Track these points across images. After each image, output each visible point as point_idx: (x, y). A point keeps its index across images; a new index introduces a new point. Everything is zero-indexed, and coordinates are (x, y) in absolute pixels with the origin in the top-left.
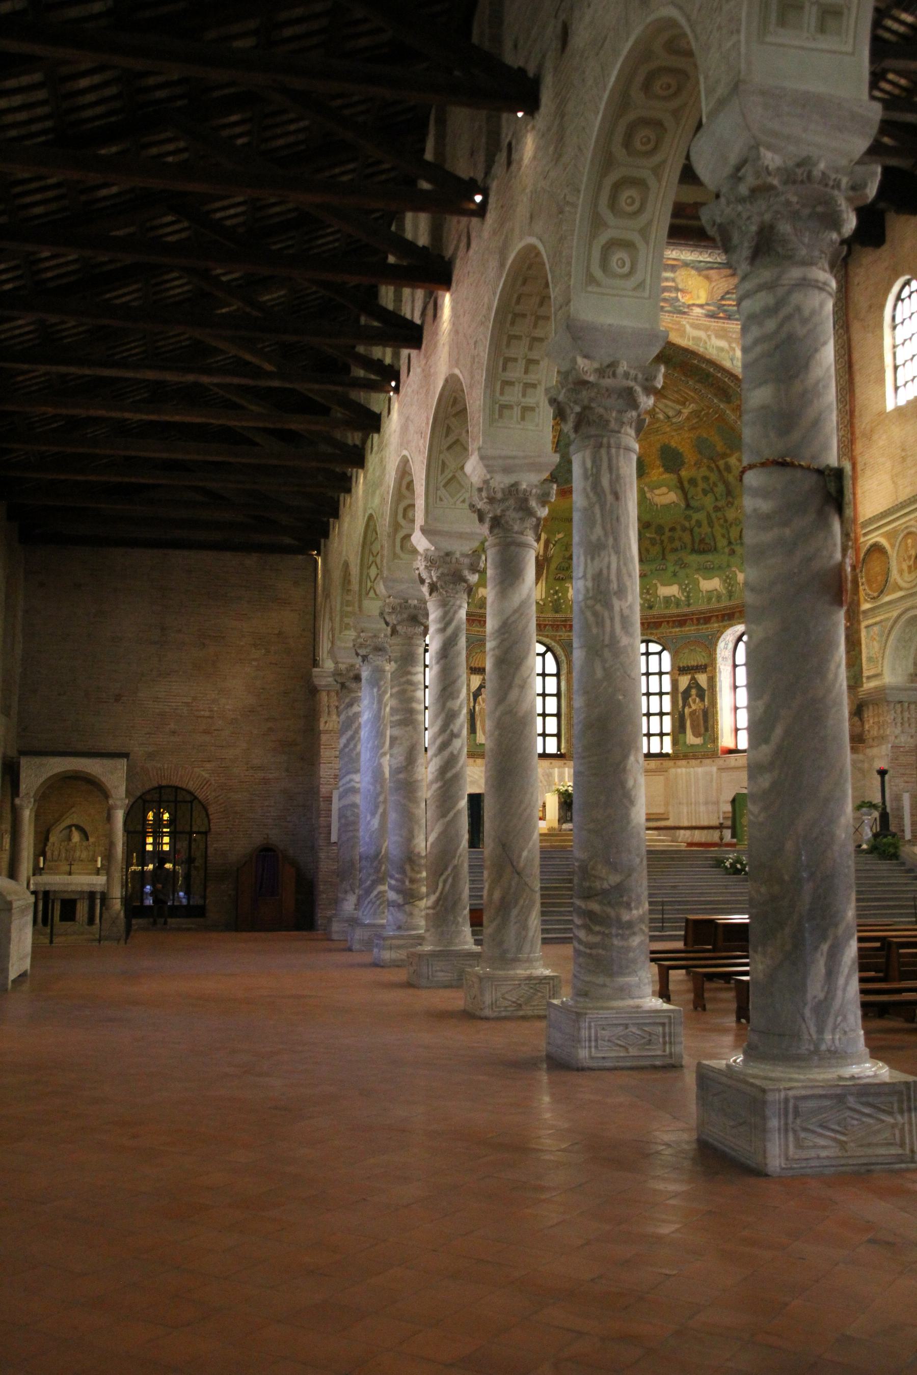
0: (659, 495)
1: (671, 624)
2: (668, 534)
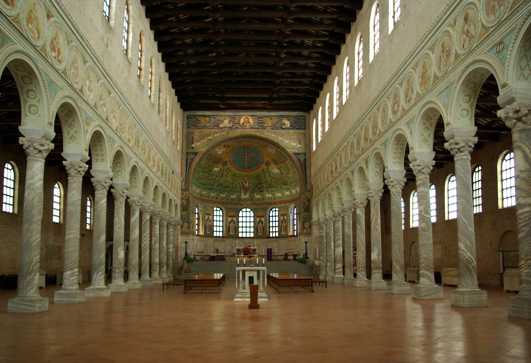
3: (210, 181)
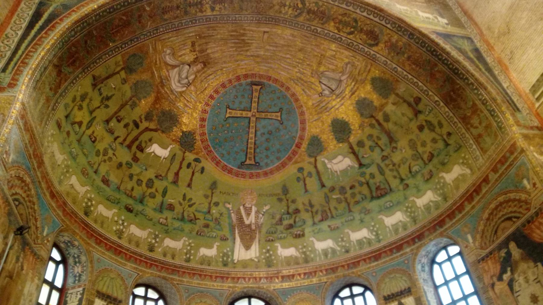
0: (336, 164)
1: (368, 261)
2: (349, 192)
3: (133, 183)
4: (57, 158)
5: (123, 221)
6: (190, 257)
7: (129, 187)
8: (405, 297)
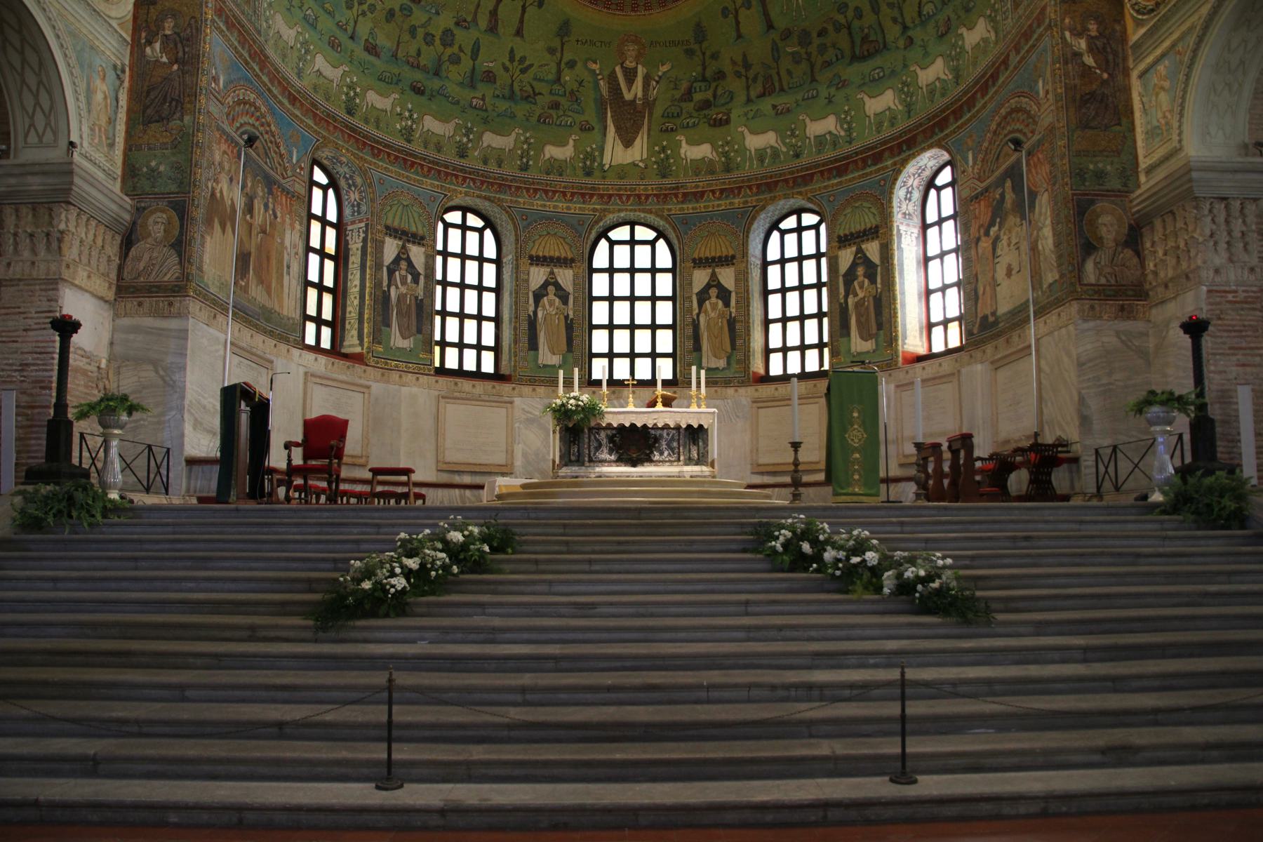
4: (285, 37)
5: (410, 111)
6: (528, 162)
7: (413, 52)
8: (868, 240)
